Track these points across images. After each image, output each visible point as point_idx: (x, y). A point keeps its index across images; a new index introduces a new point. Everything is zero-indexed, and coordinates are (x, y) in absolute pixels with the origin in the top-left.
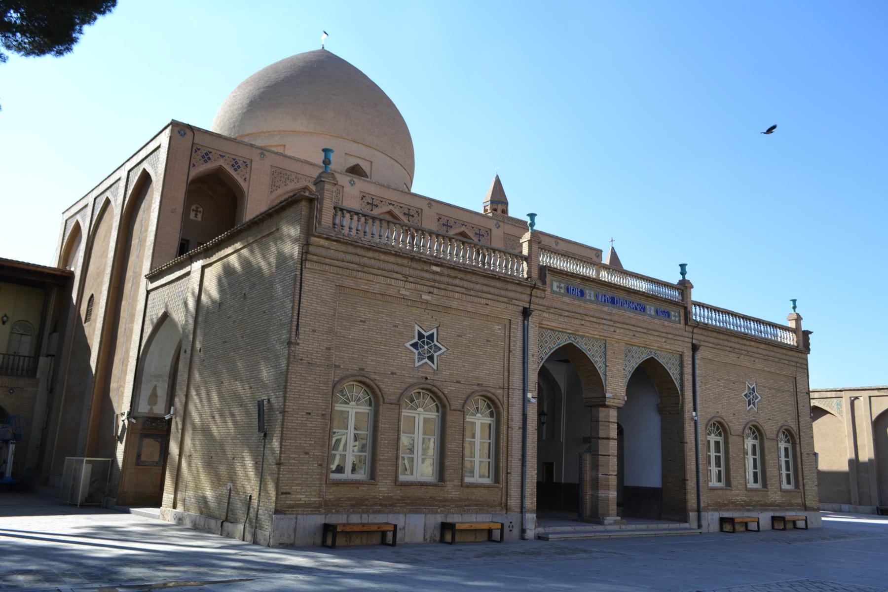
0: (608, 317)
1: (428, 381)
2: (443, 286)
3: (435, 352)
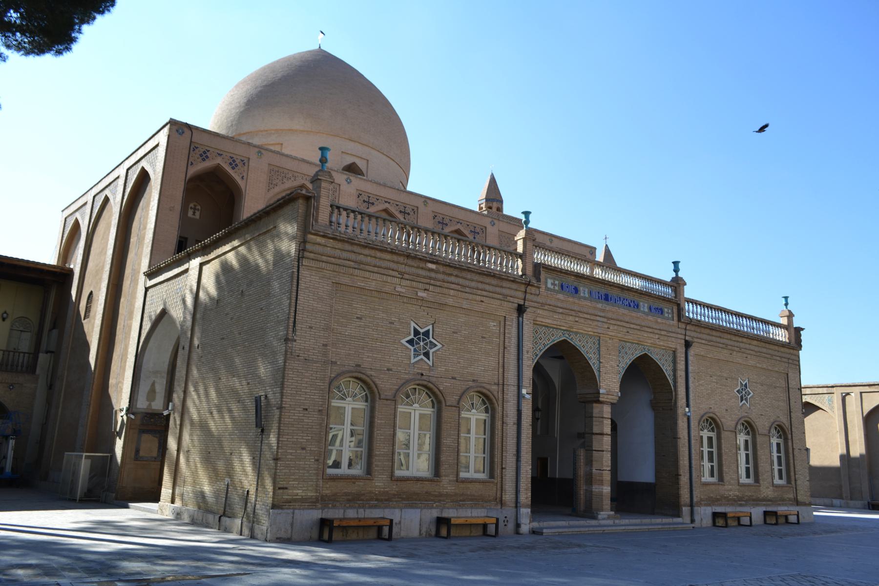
0: (602, 314)
1: (424, 378)
2: (438, 283)
3: (431, 348)
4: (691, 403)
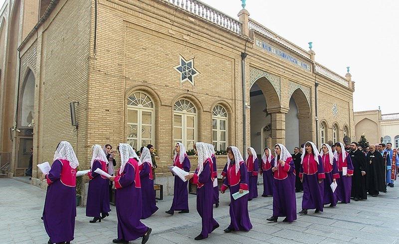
0: (282, 64)
1: (189, 92)
2: (196, 32)
3: (193, 74)
4: (318, 115)
